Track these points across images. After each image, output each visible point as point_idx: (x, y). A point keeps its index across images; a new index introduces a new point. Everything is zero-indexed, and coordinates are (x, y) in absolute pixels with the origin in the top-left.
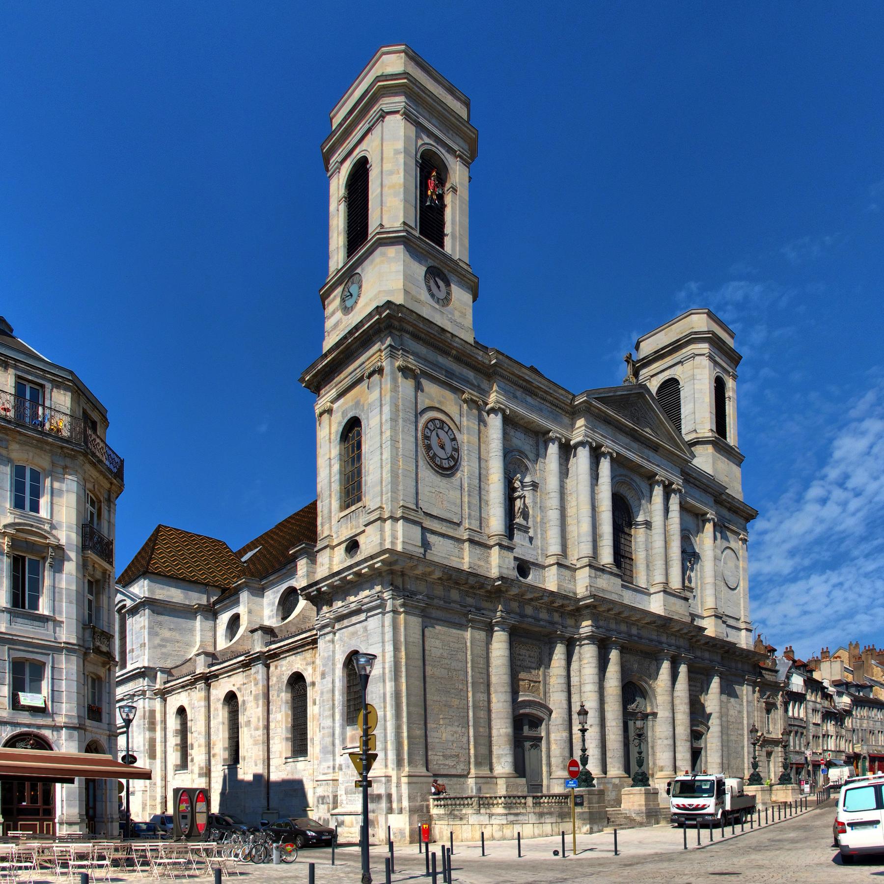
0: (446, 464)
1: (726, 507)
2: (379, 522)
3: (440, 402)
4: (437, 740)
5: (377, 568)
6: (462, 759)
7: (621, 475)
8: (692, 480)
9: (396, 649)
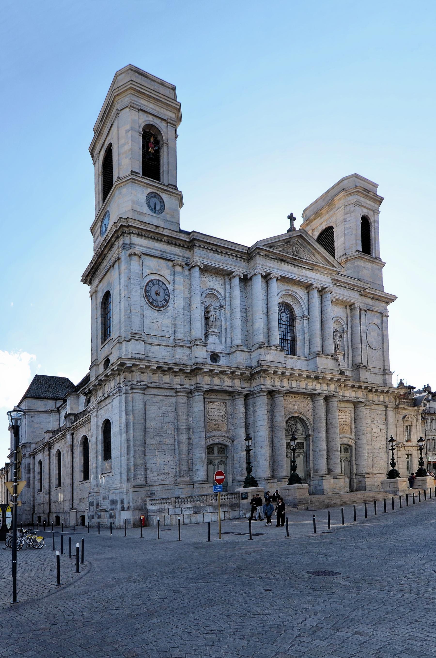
0: (160, 304)
3: (158, 270)
7: (285, 290)
9: (127, 414)
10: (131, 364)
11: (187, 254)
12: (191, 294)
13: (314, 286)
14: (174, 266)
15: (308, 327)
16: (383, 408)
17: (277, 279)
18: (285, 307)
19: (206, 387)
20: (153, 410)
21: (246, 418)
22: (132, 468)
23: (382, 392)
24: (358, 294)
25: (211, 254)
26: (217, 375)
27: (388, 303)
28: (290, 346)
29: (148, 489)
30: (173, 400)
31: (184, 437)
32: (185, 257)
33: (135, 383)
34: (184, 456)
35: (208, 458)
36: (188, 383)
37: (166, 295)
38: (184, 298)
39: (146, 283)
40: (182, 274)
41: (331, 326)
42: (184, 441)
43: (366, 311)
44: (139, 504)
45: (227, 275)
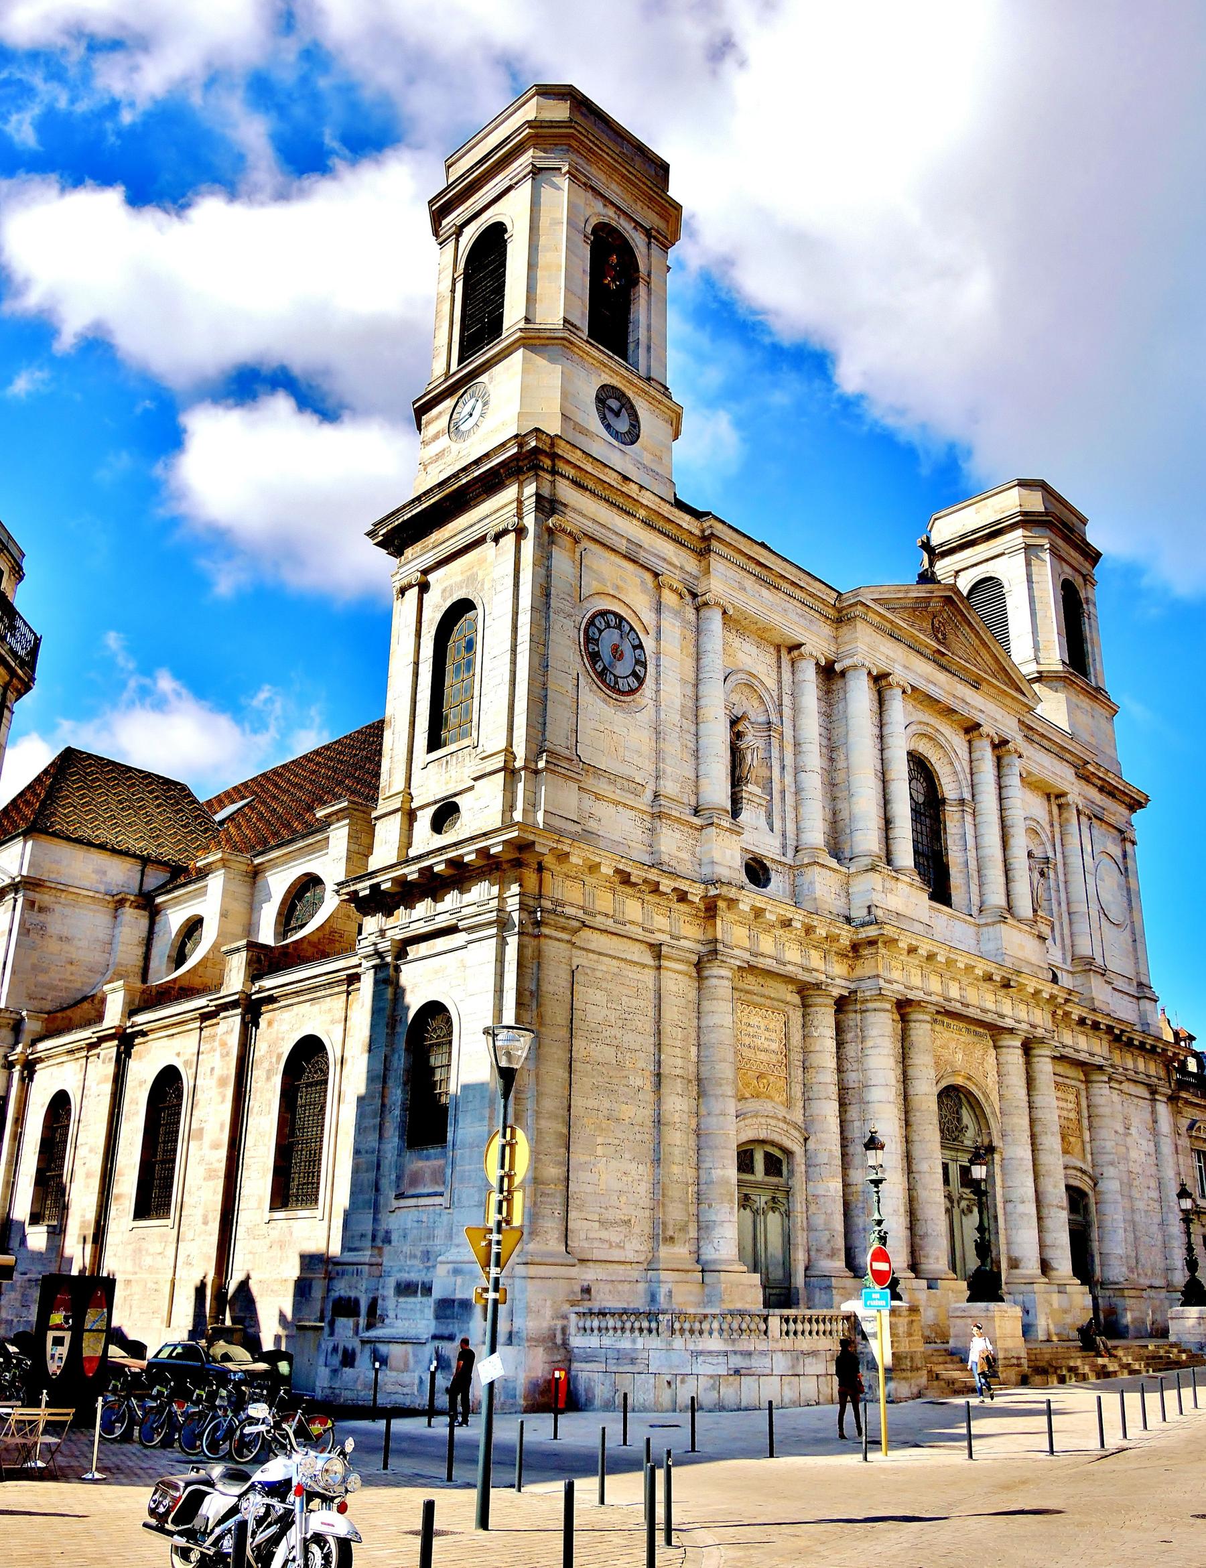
3: (618, 587)
4: (590, 1189)
5: (493, 856)
6: (637, 1230)
8: (1036, 738)
12: (701, 676)
13: (985, 729)
14: (659, 587)
15: (972, 833)
17: (904, 692)
18: (920, 766)
21: (840, 1070)
25: (749, 582)
28: (935, 876)
29: (574, 1272)
31: (677, 1105)
34: (675, 1169)
37: (638, 662)
38: (684, 681)
39: (588, 616)
40: (677, 613)
41: (1020, 843)
43: (1090, 819)
44: (545, 1325)
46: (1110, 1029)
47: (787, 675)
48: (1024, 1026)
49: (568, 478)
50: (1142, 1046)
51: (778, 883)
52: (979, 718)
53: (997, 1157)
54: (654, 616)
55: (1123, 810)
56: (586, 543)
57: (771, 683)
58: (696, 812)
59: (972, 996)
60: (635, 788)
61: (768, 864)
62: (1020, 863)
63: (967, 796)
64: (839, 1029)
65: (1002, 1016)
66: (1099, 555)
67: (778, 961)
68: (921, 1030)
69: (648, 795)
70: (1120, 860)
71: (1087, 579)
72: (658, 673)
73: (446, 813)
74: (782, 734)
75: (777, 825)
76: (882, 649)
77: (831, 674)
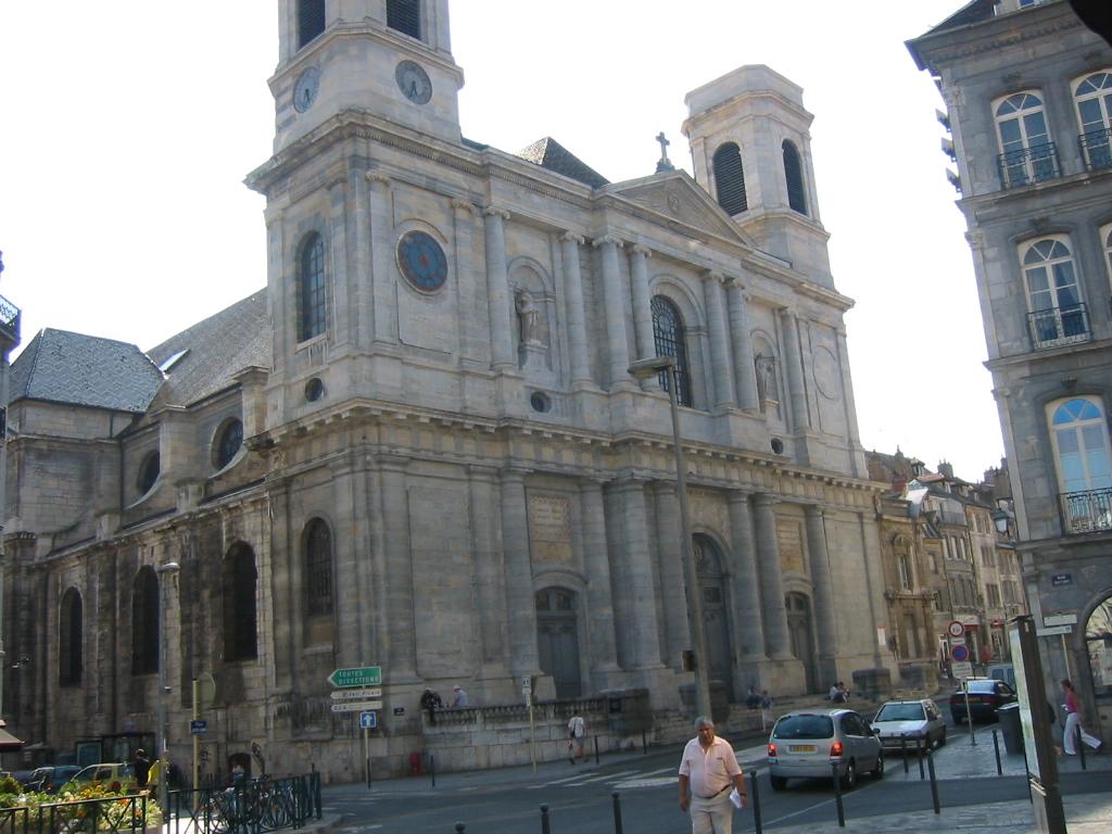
1: (811, 297)
2: (346, 361)
3: (421, 213)
8: (759, 270)
10: (379, 410)
11: (478, 186)
14: (453, 207)
16: (855, 518)
18: (663, 304)
19: (526, 465)
20: (423, 510)
22: (386, 639)
23: (849, 486)
24: (791, 290)
26: (546, 441)
27: (843, 310)
30: (464, 487)
32: (474, 193)
33: (385, 449)
35: (539, 619)
36: (494, 453)
41: (749, 348)
42: (489, 580)
43: (807, 323)
45: (556, 235)
46: (820, 479)
47: (557, 256)
48: (749, 486)
49: (377, 140)
50: (849, 486)
51: (556, 404)
52: (707, 265)
53: (731, 580)
54: (451, 228)
55: (836, 312)
56: (393, 184)
57: (545, 262)
58: (492, 367)
59: (706, 471)
60: (443, 356)
61: (547, 394)
62: (749, 363)
63: (702, 324)
64: (607, 506)
65: (730, 481)
66: (812, 117)
67: (558, 465)
68: (669, 501)
69: (456, 361)
70: (834, 351)
71: (805, 137)
72: (456, 269)
73: (314, 389)
74: (554, 298)
75: (556, 365)
76: (628, 226)
77: (591, 248)
